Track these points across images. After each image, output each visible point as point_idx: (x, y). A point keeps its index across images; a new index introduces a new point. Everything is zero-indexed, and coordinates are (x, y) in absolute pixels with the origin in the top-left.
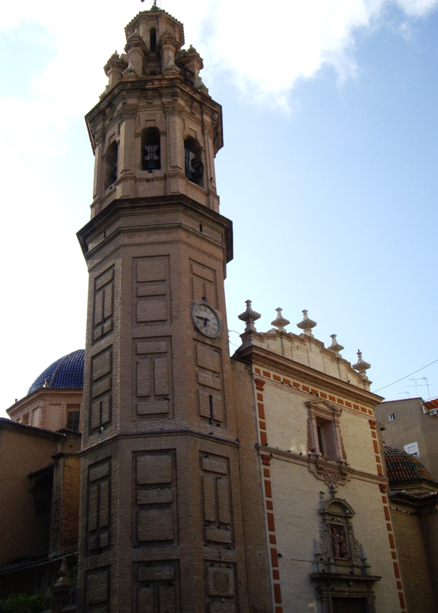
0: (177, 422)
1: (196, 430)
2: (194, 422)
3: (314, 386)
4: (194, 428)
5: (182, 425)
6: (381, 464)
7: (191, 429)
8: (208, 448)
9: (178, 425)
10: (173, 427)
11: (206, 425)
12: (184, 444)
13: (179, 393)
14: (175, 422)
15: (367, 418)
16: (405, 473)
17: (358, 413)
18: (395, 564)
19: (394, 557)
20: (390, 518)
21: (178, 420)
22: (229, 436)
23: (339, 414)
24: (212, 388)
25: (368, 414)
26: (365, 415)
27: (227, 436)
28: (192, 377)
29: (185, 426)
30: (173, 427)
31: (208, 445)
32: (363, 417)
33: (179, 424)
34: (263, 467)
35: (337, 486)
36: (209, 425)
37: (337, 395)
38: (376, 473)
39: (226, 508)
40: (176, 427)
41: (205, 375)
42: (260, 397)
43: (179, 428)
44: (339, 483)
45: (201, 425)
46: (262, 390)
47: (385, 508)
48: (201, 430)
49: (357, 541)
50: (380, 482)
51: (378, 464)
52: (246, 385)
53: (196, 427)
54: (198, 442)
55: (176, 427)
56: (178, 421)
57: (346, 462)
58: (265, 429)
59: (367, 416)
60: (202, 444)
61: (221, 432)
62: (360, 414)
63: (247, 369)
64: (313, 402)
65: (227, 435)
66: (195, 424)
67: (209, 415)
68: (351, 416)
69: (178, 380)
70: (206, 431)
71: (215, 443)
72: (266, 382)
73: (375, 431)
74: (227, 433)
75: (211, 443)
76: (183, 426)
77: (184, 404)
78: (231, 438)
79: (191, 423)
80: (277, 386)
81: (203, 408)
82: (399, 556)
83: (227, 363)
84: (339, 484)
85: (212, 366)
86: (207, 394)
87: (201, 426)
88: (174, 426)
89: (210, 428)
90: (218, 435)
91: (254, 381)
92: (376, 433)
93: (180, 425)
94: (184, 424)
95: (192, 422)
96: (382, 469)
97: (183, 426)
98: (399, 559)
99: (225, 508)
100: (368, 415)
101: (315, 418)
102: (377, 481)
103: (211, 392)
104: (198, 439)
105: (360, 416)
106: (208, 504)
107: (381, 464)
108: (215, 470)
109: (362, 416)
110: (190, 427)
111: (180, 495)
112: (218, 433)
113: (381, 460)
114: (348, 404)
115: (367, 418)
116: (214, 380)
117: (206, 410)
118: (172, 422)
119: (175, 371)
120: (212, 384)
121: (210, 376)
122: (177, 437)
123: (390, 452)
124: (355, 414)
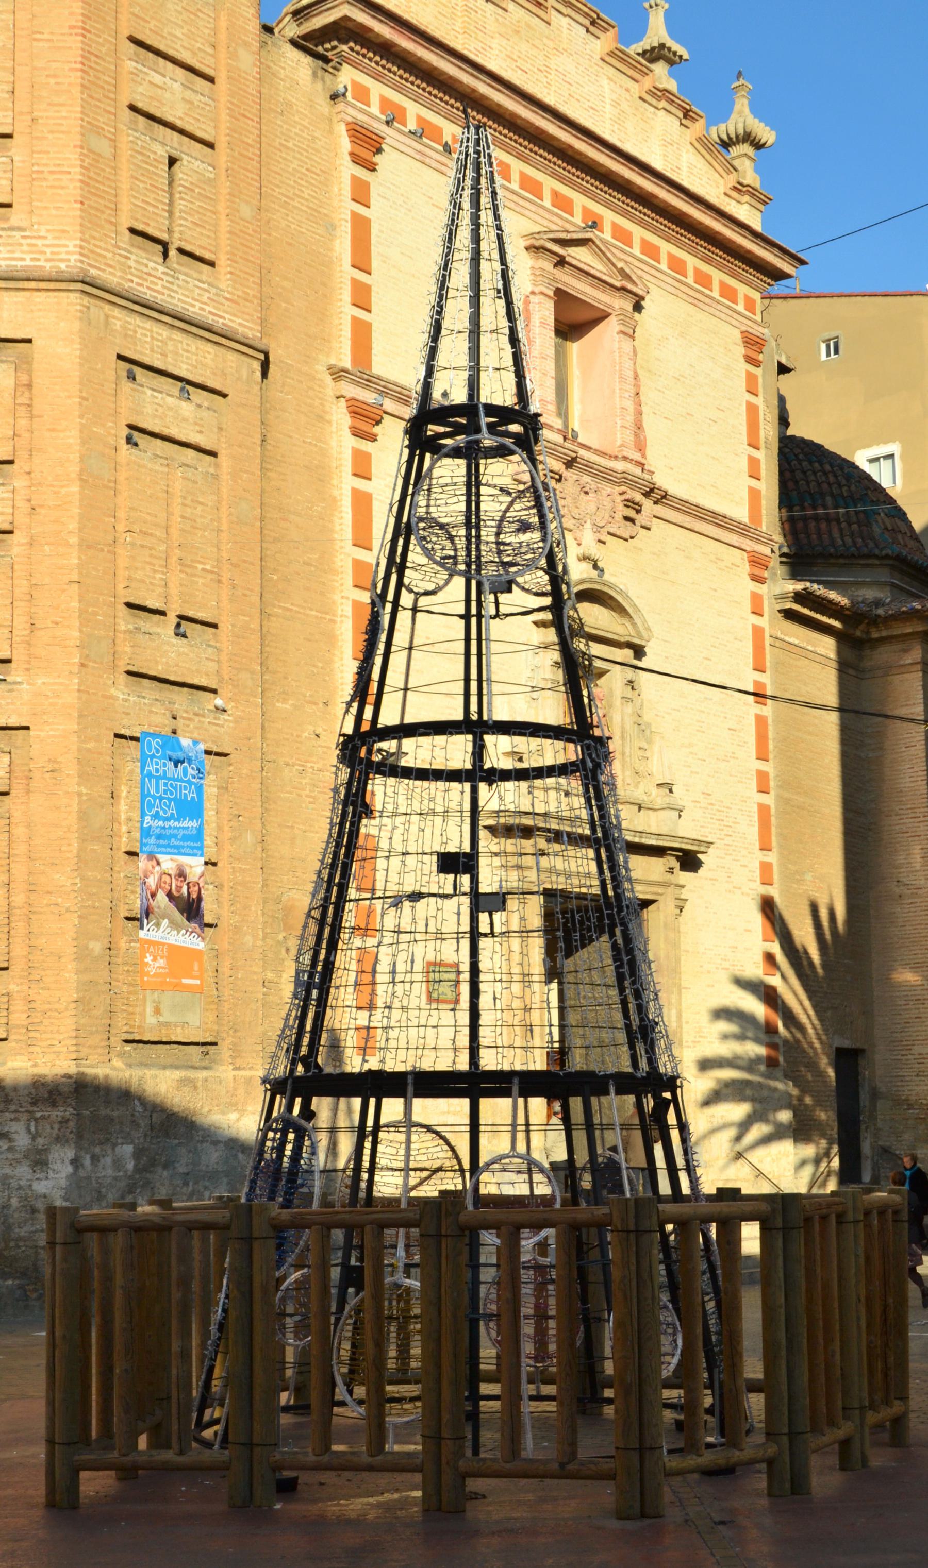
0: (39, 242)
1: (110, 277)
2: (106, 250)
3: (561, 179)
4: (103, 271)
5: (58, 253)
6: (761, 486)
7: (93, 272)
8: (152, 350)
9: (45, 253)
10: (23, 259)
11: (151, 264)
12: (62, 324)
13: (52, 132)
14: (33, 241)
15: (734, 322)
16: (841, 530)
17: (707, 300)
18: (764, 811)
19: (763, 789)
20: (768, 664)
21: (42, 234)
22: (235, 316)
23: (640, 293)
24: (182, 132)
25: (740, 307)
26: (730, 313)
27: (227, 316)
28: (107, 79)
29: (69, 260)
30: (23, 259)
31: (152, 338)
32: (723, 316)
33: (48, 250)
34: (351, 442)
35: (602, 539)
36: (161, 269)
37: (641, 223)
38: (741, 513)
39: (208, 567)
40: (39, 260)
41: (157, 79)
42: (361, 195)
43: (48, 265)
44: (612, 531)
45: (131, 263)
46: (372, 168)
47: (758, 632)
48: (132, 281)
49: (649, 725)
50: (750, 543)
51: (753, 483)
52: (314, 138)
53: (110, 266)
54: (118, 324)
55: (39, 260)
56: (45, 238)
57: (643, 461)
58: (370, 311)
59: (735, 316)
60: (131, 333)
61: (205, 299)
62: (714, 305)
63: (323, 80)
64: (552, 236)
65: (225, 312)
66: (109, 255)
67: (163, 231)
68: (680, 309)
69: (52, 81)
70: (148, 288)
71: (178, 336)
72: (388, 140)
73: (758, 372)
74: (227, 303)
75: (165, 332)
76: (62, 260)
77: (69, 177)
78: (240, 324)
79: (92, 252)
80: (428, 161)
81: (143, 201)
82: (779, 787)
83: (246, 44)
84: (609, 533)
85: (184, 48)
86: (162, 153)
87: (130, 267)
88: (28, 257)
89: (166, 278)
90: (193, 306)
91: (342, 128)
92: (760, 380)
93: (52, 253)
94: (68, 253)
95: (99, 247)
96: (764, 502)
97: (62, 260)
98: (778, 797)
99: (200, 566)
100: (739, 313)
101: (551, 293)
102: (742, 539)
103: (176, 145)
104: (117, 312)
105: (712, 310)
106: (142, 546)
107: (761, 486)
108: (174, 432)
109: (717, 313)
110: (89, 265)
111: (42, 506)
112: (193, 299)
113: (763, 473)
114: (677, 266)
115: (734, 322)
116: (191, 103)
117: (151, 209)
118: (23, 241)
119: (41, 44)
120: (180, 114)
121: (176, 86)
122: (39, 297)
123: (801, 456)
124: (695, 303)
